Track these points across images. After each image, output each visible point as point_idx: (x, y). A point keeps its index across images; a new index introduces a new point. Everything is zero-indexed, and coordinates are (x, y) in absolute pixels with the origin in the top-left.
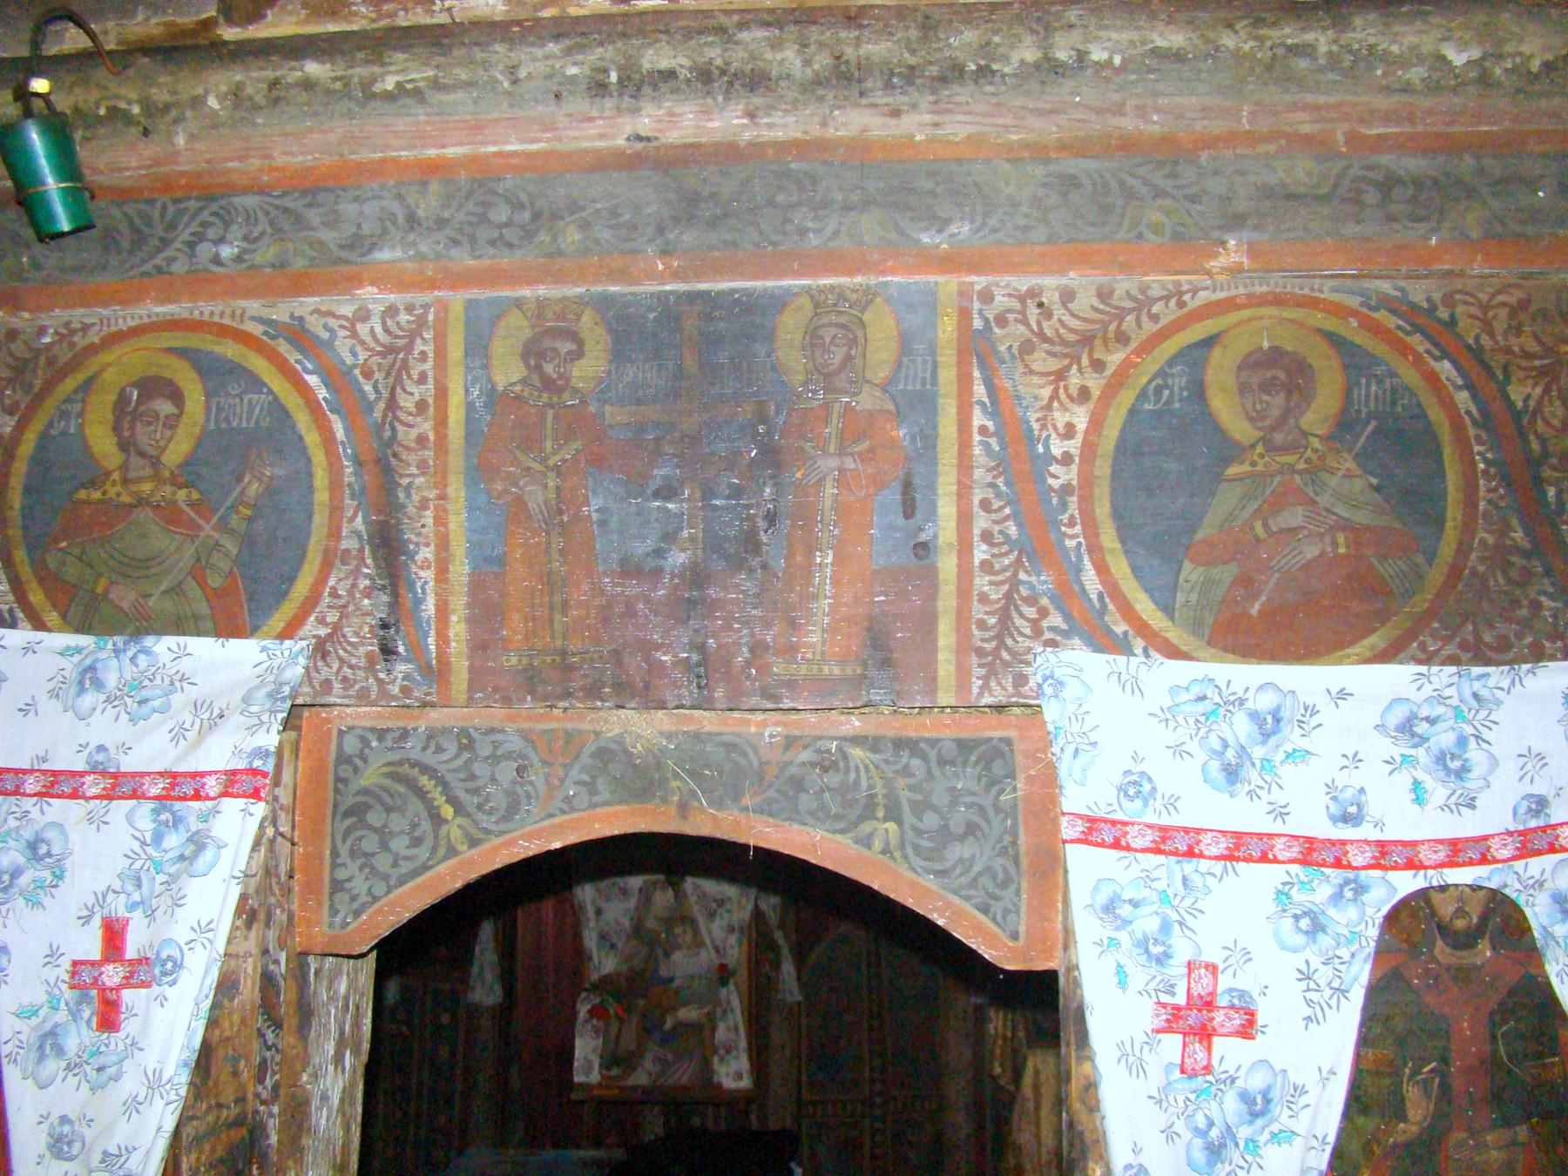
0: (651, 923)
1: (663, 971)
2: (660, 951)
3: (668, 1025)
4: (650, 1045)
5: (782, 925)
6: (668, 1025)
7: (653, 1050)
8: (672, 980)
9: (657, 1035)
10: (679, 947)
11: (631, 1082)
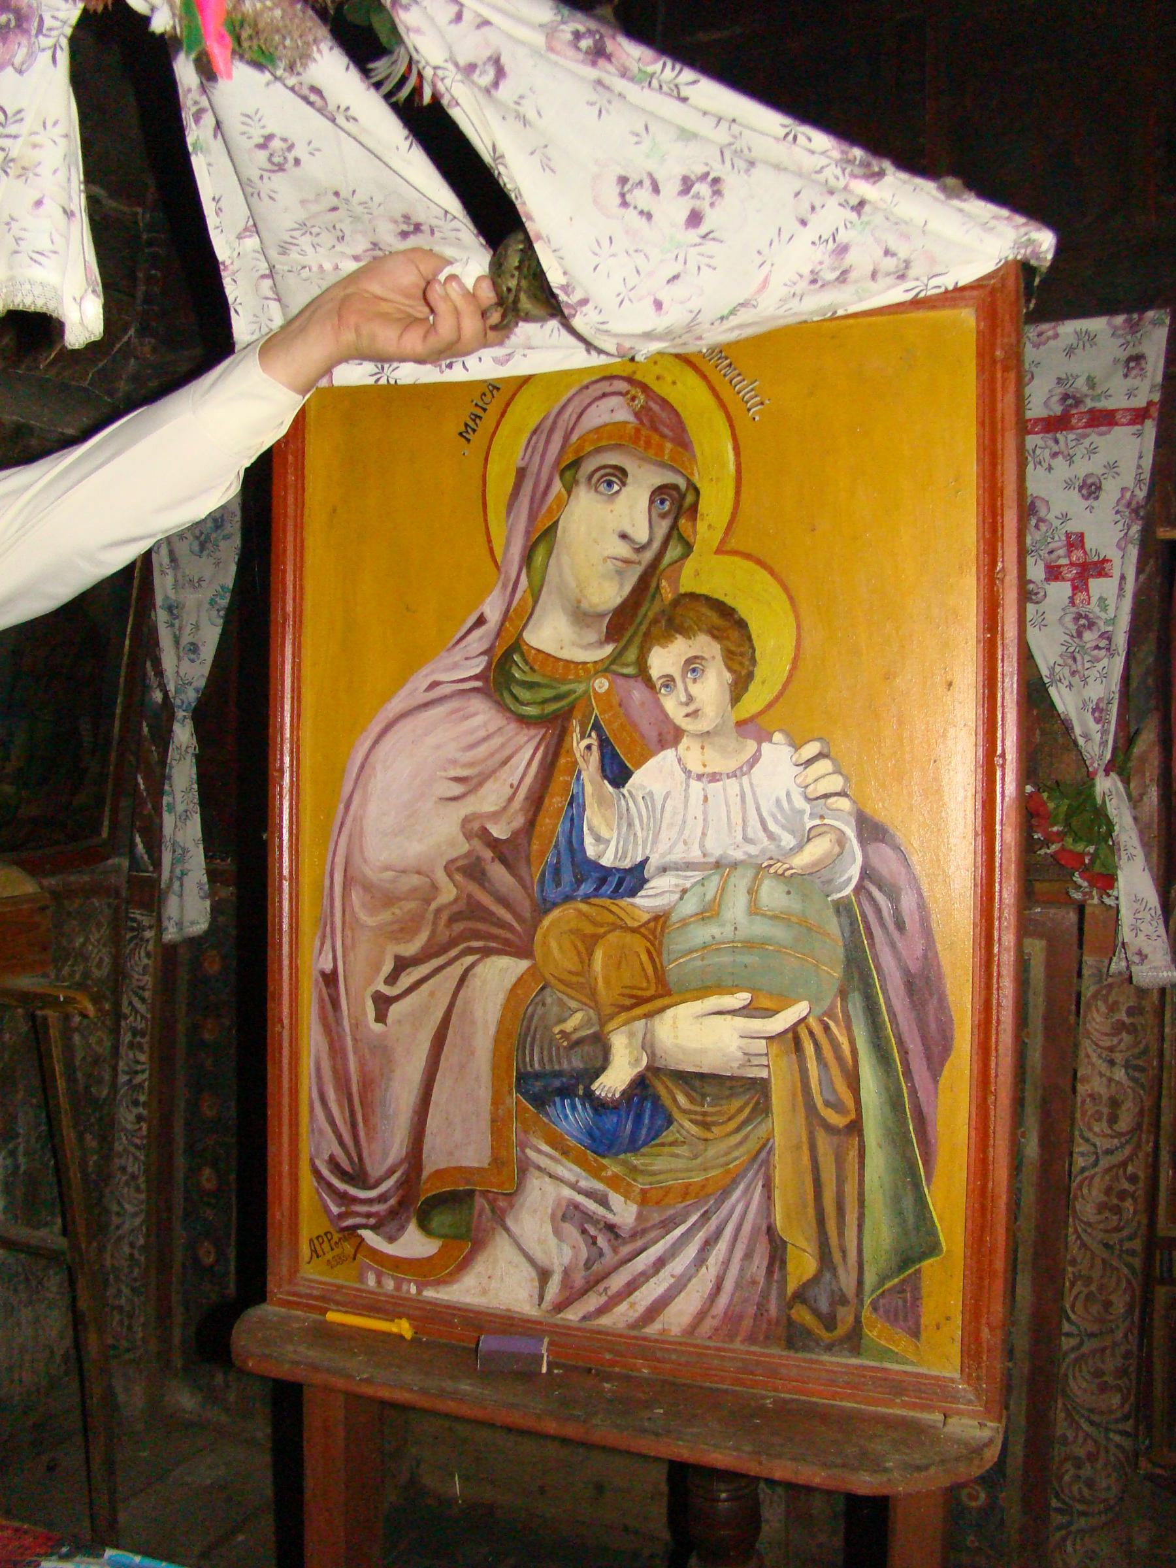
0: (551, 634)
1: (605, 846)
2: (582, 747)
3: (614, 1081)
4: (540, 1152)
5: (1118, 765)
6: (614, 1081)
7: (552, 1185)
8: (632, 879)
9: (572, 1119)
10: (671, 736)
11: (466, 1291)
